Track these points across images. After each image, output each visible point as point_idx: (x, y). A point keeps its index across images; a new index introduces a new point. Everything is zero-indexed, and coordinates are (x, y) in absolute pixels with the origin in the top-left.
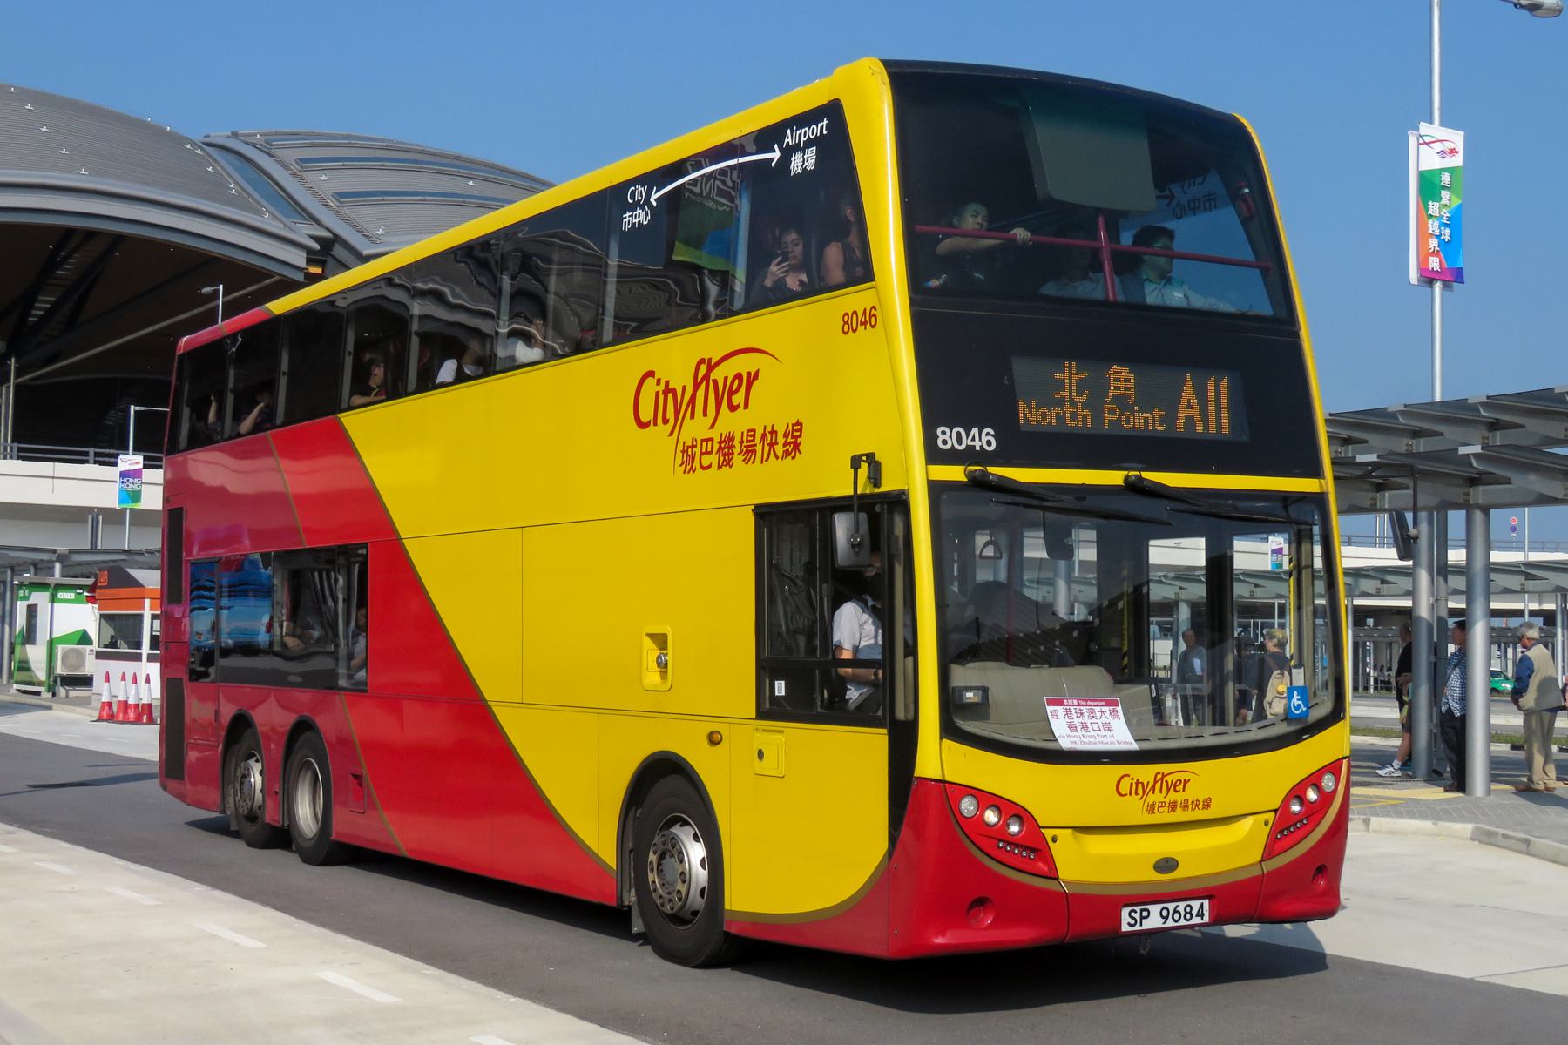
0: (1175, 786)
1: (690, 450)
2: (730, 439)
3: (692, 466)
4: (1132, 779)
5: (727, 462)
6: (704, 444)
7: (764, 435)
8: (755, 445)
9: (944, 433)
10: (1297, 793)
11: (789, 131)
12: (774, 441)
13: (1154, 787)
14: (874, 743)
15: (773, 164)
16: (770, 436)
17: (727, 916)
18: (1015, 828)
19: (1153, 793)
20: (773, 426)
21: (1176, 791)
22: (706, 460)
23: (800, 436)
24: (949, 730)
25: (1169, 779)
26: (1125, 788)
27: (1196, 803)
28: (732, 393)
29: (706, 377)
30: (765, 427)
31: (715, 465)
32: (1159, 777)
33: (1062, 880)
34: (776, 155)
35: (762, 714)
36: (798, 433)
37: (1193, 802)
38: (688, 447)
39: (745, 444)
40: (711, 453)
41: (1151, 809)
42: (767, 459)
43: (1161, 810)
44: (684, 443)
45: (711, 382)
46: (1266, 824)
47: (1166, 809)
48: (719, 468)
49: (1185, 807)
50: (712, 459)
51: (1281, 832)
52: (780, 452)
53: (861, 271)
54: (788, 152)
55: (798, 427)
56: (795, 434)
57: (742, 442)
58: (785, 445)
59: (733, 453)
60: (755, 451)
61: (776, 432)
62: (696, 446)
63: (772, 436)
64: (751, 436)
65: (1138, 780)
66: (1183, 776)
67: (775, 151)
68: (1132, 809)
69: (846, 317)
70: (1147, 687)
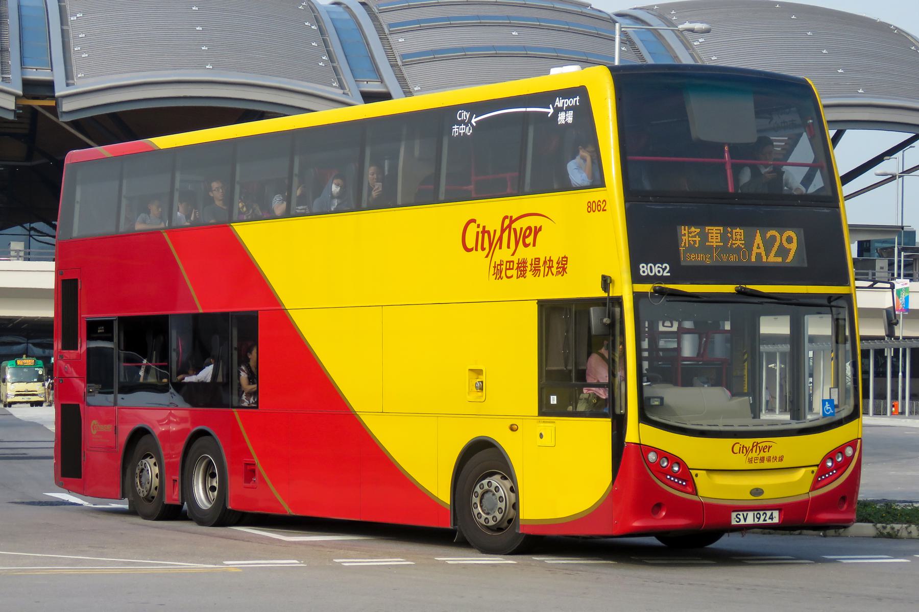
0: (764, 449)
1: (499, 267)
2: (525, 262)
3: (500, 276)
4: (741, 445)
5: (522, 273)
6: (508, 264)
7: (545, 262)
8: (540, 267)
9: (643, 267)
10: (831, 456)
11: (558, 98)
12: (551, 265)
13: (752, 450)
14: (604, 426)
15: (549, 115)
16: (548, 262)
17: (521, 523)
18: (676, 469)
19: (752, 452)
20: (550, 257)
21: (764, 452)
22: (509, 273)
23: (566, 264)
24: (644, 418)
25: (760, 445)
26: (736, 449)
27: (775, 458)
28: (525, 237)
29: (509, 226)
30: (546, 257)
31: (515, 276)
32: (755, 444)
33: (701, 497)
34: (551, 111)
35: (542, 413)
36: (565, 263)
37: (773, 458)
38: (498, 265)
39: (533, 266)
40: (513, 269)
41: (750, 461)
42: (547, 276)
43: (755, 461)
44: (495, 262)
45: (512, 230)
46: (813, 472)
47: (759, 461)
48: (517, 278)
49: (769, 460)
50: (514, 272)
51: (821, 477)
52: (555, 273)
53: (598, 181)
54: (558, 110)
55: (565, 259)
56: (563, 263)
57: (531, 265)
58: (557, 268)
59: (526, 270)
60: (540, 270)
61: (552, 261)
62: (503, 265)
63: (550, 263)
64: (537, 261)
65: (743, 447)
66: (768, 444)
67: (550, 108)
68: (740, 462)
69: (589, 204)
70: (748, 398)
